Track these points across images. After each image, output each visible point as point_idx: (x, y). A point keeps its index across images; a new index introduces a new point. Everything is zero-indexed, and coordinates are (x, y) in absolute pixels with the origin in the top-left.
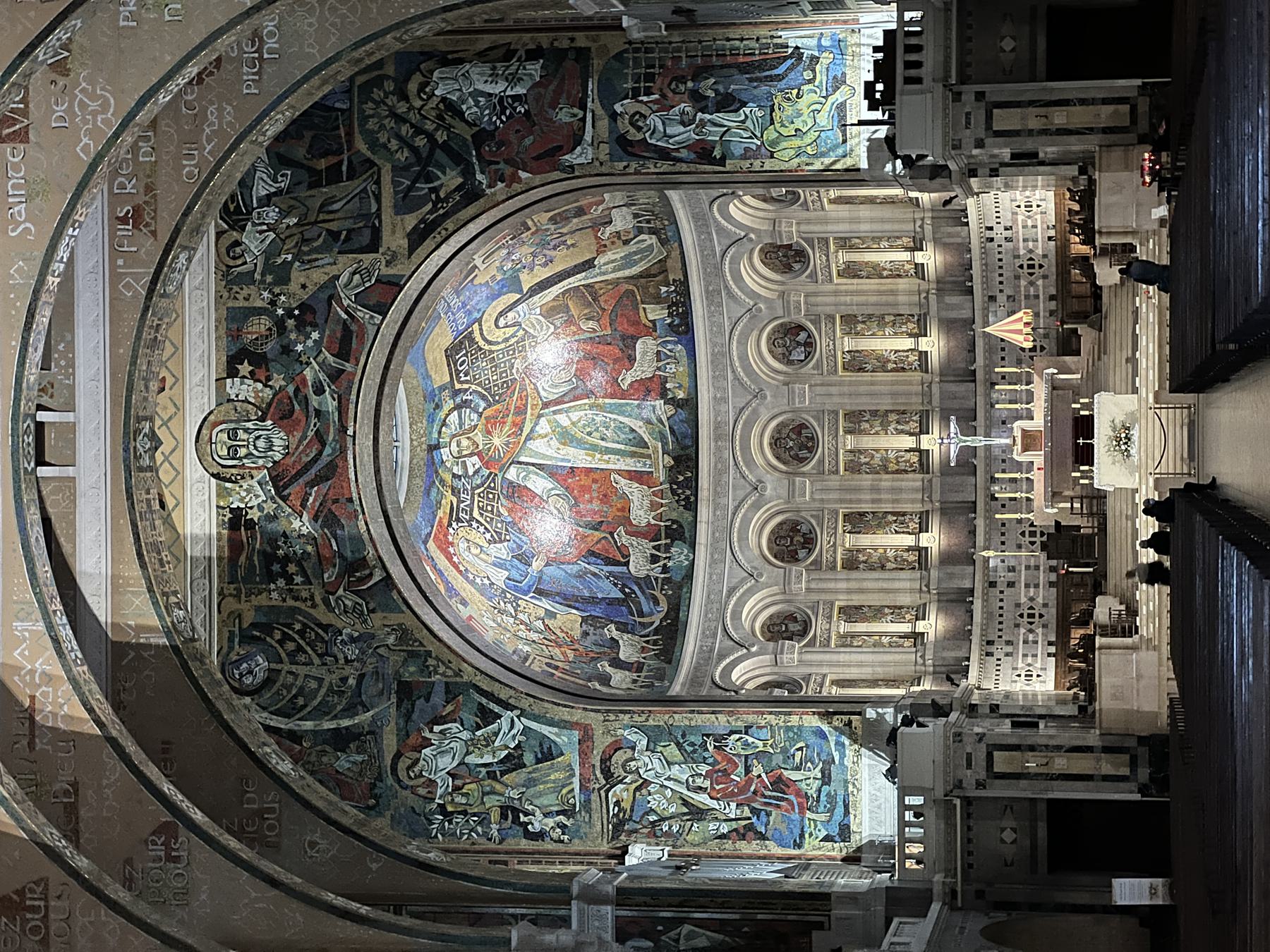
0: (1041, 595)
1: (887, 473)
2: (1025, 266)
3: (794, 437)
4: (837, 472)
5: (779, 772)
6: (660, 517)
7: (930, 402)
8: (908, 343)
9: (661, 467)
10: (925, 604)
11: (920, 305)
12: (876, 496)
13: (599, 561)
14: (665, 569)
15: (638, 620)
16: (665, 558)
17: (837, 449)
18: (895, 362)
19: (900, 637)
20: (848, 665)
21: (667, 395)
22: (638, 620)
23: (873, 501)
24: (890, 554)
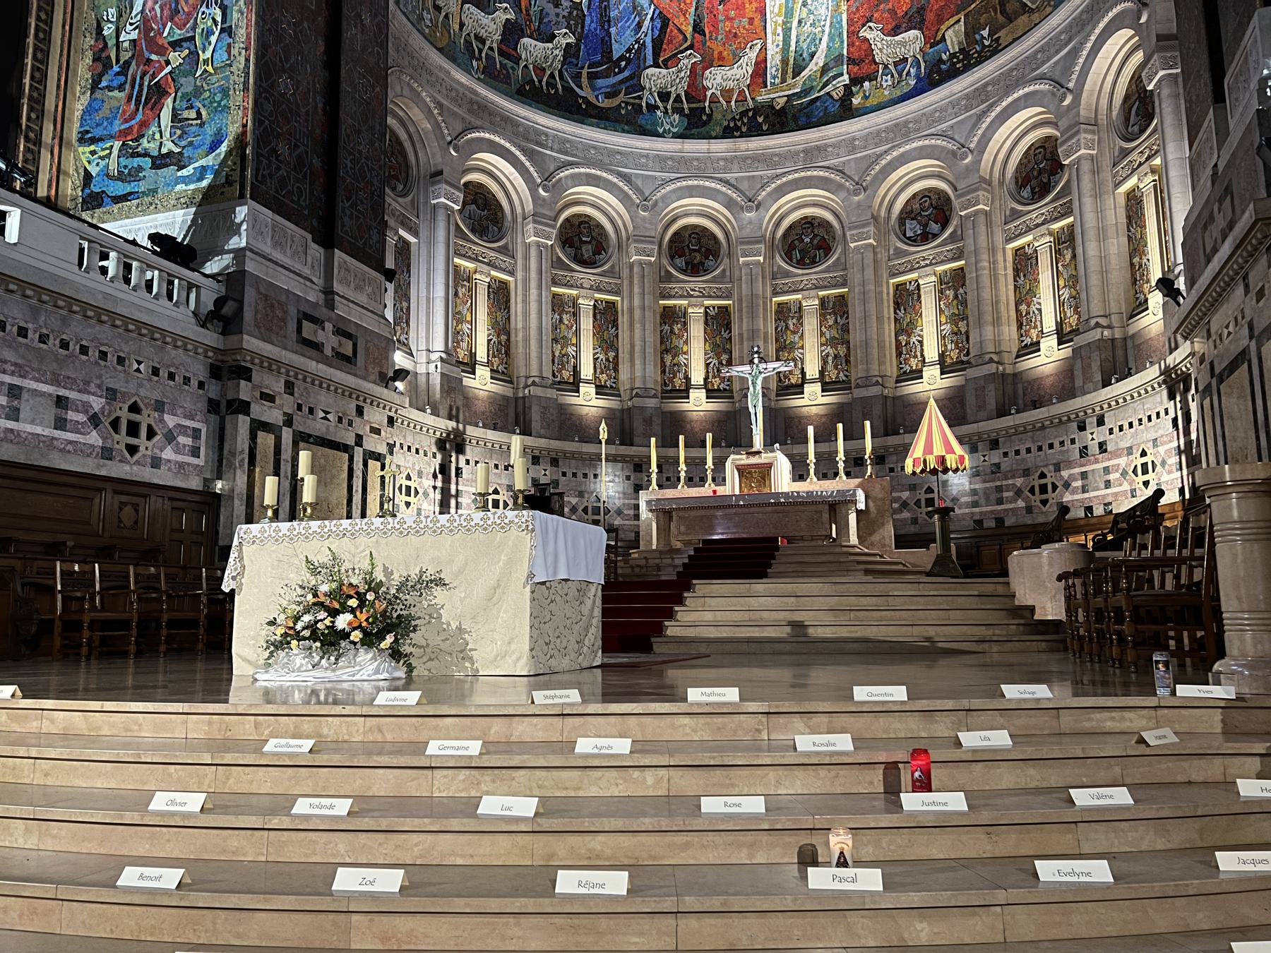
0: (627, 522)
1: (777, 351)
2: (1043, 481)
3: (815, 242)
4: (775, 294)
5: (172, 91)
6: (714, 99)
7: (858, 386)
8: (931, 353)
9: (772, 96)
10: (619, 396)
11: (980, 356)
12: (745, 336)
13: (657, 33)
14: (652, 108)
15: (585, 72)
16: (666, 108)
17: (802, 290)
18: (908, 343)
19: (575, 367)
20: (526, 302)
21: (855, 85)
22: (585, 72)
23: (741, 335)
24: (682, 359)
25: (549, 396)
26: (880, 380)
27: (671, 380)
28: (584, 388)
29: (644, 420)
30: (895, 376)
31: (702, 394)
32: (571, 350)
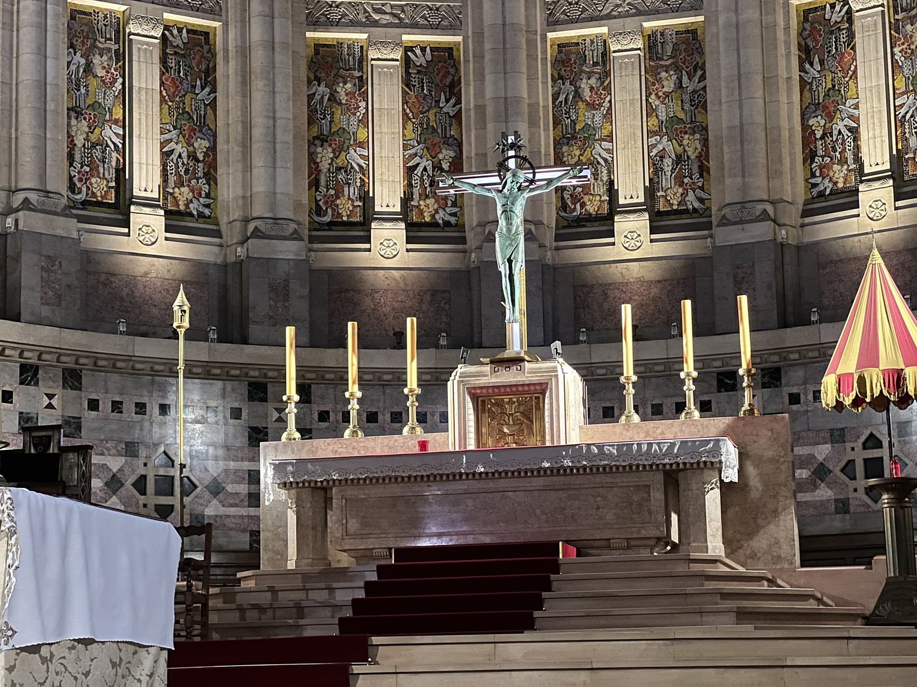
0: (232, 511)
1: (557, 144)
4: (553, 23)
7: (725, 222)
10: (218, 234)
12: (490, 110)
17: (609, 17)
19: (120, 171)
23: (481, 109)
24: (355, 157)
25: (60, 232)
26: (770, 209)
27: (331, 202)
28: (140, 217)
29: (273, 288)
30: (801, 198)
31: (397, 233)
32: (111, 134)
